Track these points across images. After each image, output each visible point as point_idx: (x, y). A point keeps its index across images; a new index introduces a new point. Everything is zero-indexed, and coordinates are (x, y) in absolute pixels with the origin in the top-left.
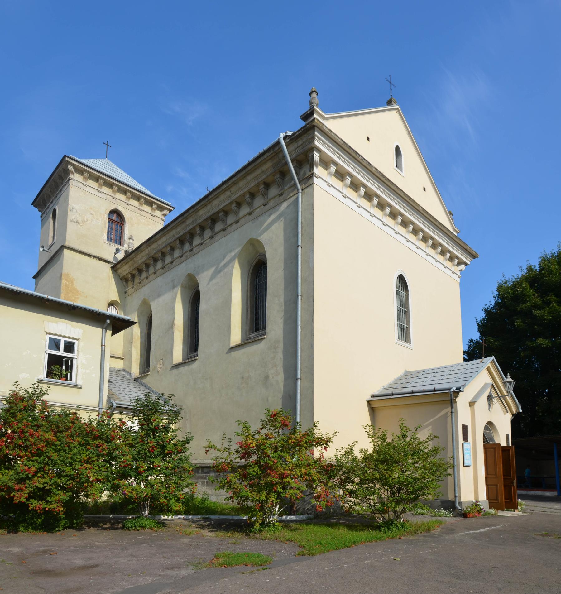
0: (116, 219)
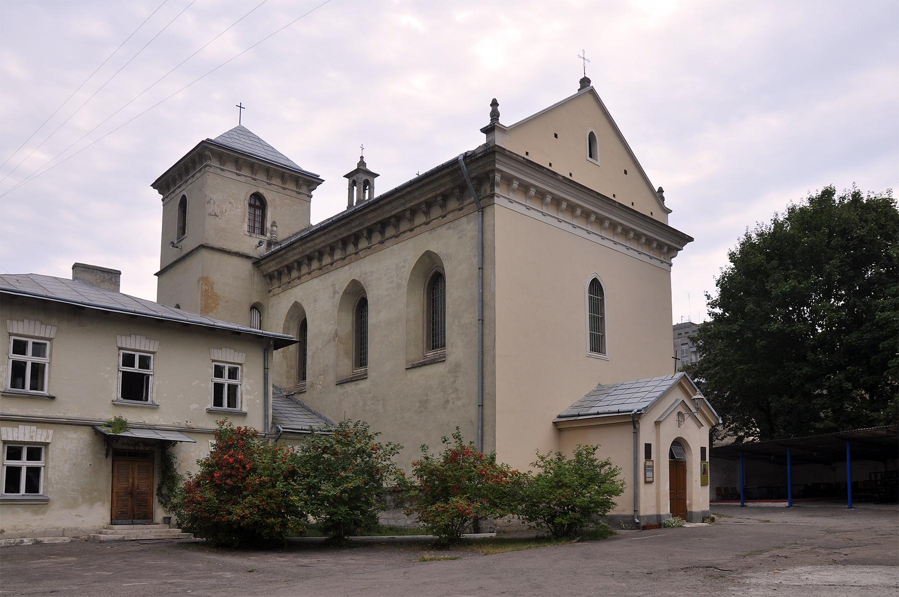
0: (258, 203)
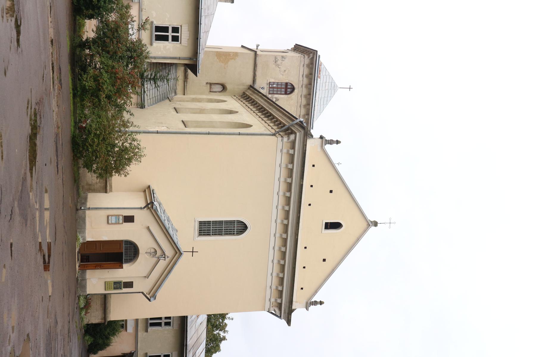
0: (289, 89)
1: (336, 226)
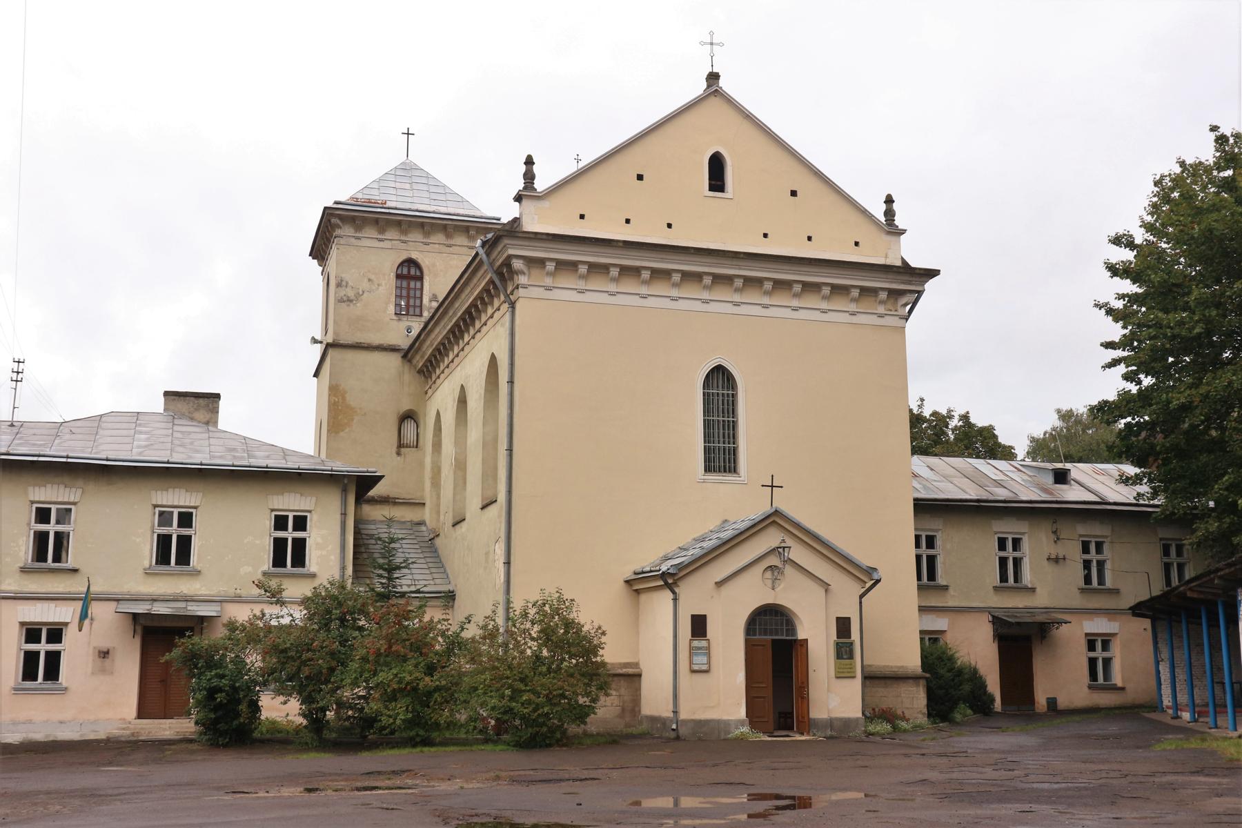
0: (410, 273)
1: (717, 166)
